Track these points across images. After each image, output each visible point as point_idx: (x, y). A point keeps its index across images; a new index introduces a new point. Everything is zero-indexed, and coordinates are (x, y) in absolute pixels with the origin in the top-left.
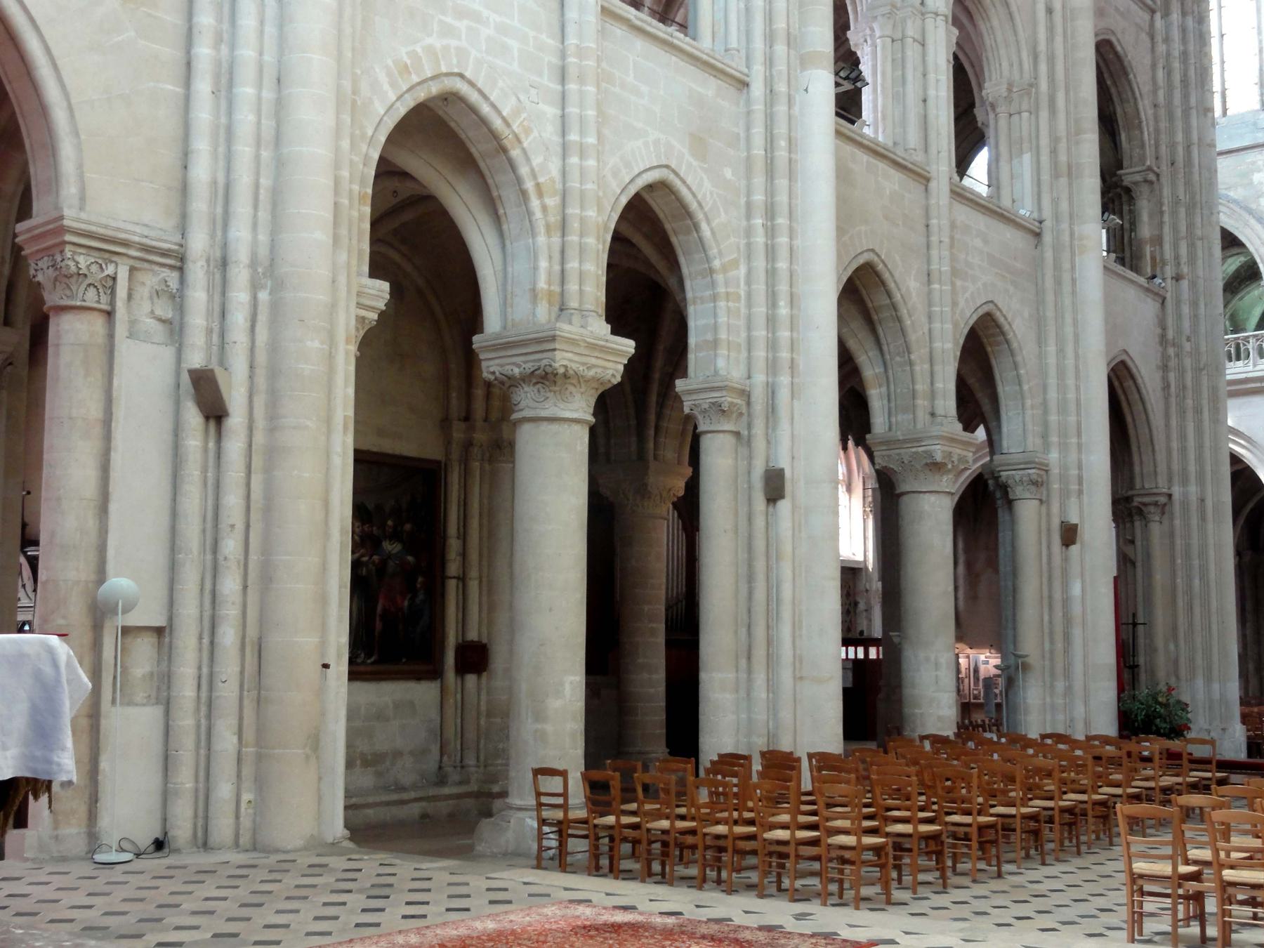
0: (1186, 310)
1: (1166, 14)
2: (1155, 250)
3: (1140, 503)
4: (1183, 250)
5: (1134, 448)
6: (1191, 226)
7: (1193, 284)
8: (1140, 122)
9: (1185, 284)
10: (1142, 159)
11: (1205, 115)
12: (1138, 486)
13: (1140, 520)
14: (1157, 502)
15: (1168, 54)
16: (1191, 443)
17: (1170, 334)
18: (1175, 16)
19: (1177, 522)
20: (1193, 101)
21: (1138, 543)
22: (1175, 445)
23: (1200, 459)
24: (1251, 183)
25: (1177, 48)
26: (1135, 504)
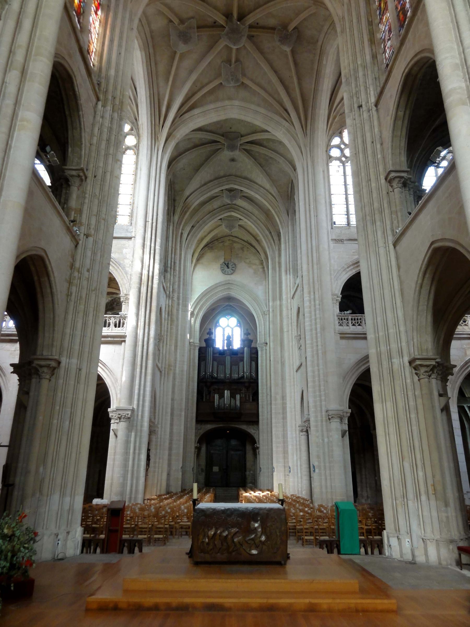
0: (89, 253)
1: (104, 106)
2: (77, 216)
3: (38, 365)
4: (93, 221)
5: (40, 328)
6: (99, 212)
7: (95, 242)
8: (82, 144)
9: (91, 239)
10: (79, 164)
11: (116, 162)
12: (38, 353)
13: (36, 378)
14: (50, 365)
15: (102, 125)
16: (78, 333)
17: (77, 265)
18: (109, 108)
19: (61, 381)
20: (111, 152)
21: (31, 394)
22: (68, 331)
23: (82, 344)
24: (122, 253)
25: (107, 123)
26: (34, 365)
